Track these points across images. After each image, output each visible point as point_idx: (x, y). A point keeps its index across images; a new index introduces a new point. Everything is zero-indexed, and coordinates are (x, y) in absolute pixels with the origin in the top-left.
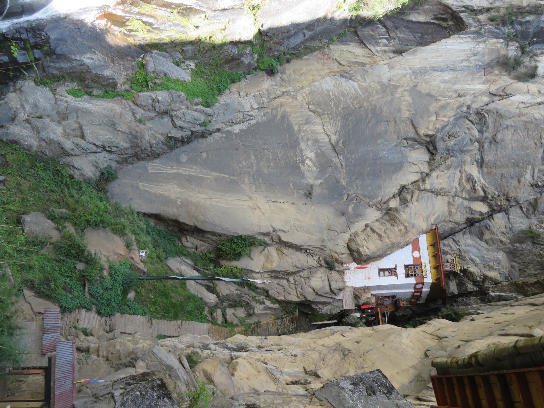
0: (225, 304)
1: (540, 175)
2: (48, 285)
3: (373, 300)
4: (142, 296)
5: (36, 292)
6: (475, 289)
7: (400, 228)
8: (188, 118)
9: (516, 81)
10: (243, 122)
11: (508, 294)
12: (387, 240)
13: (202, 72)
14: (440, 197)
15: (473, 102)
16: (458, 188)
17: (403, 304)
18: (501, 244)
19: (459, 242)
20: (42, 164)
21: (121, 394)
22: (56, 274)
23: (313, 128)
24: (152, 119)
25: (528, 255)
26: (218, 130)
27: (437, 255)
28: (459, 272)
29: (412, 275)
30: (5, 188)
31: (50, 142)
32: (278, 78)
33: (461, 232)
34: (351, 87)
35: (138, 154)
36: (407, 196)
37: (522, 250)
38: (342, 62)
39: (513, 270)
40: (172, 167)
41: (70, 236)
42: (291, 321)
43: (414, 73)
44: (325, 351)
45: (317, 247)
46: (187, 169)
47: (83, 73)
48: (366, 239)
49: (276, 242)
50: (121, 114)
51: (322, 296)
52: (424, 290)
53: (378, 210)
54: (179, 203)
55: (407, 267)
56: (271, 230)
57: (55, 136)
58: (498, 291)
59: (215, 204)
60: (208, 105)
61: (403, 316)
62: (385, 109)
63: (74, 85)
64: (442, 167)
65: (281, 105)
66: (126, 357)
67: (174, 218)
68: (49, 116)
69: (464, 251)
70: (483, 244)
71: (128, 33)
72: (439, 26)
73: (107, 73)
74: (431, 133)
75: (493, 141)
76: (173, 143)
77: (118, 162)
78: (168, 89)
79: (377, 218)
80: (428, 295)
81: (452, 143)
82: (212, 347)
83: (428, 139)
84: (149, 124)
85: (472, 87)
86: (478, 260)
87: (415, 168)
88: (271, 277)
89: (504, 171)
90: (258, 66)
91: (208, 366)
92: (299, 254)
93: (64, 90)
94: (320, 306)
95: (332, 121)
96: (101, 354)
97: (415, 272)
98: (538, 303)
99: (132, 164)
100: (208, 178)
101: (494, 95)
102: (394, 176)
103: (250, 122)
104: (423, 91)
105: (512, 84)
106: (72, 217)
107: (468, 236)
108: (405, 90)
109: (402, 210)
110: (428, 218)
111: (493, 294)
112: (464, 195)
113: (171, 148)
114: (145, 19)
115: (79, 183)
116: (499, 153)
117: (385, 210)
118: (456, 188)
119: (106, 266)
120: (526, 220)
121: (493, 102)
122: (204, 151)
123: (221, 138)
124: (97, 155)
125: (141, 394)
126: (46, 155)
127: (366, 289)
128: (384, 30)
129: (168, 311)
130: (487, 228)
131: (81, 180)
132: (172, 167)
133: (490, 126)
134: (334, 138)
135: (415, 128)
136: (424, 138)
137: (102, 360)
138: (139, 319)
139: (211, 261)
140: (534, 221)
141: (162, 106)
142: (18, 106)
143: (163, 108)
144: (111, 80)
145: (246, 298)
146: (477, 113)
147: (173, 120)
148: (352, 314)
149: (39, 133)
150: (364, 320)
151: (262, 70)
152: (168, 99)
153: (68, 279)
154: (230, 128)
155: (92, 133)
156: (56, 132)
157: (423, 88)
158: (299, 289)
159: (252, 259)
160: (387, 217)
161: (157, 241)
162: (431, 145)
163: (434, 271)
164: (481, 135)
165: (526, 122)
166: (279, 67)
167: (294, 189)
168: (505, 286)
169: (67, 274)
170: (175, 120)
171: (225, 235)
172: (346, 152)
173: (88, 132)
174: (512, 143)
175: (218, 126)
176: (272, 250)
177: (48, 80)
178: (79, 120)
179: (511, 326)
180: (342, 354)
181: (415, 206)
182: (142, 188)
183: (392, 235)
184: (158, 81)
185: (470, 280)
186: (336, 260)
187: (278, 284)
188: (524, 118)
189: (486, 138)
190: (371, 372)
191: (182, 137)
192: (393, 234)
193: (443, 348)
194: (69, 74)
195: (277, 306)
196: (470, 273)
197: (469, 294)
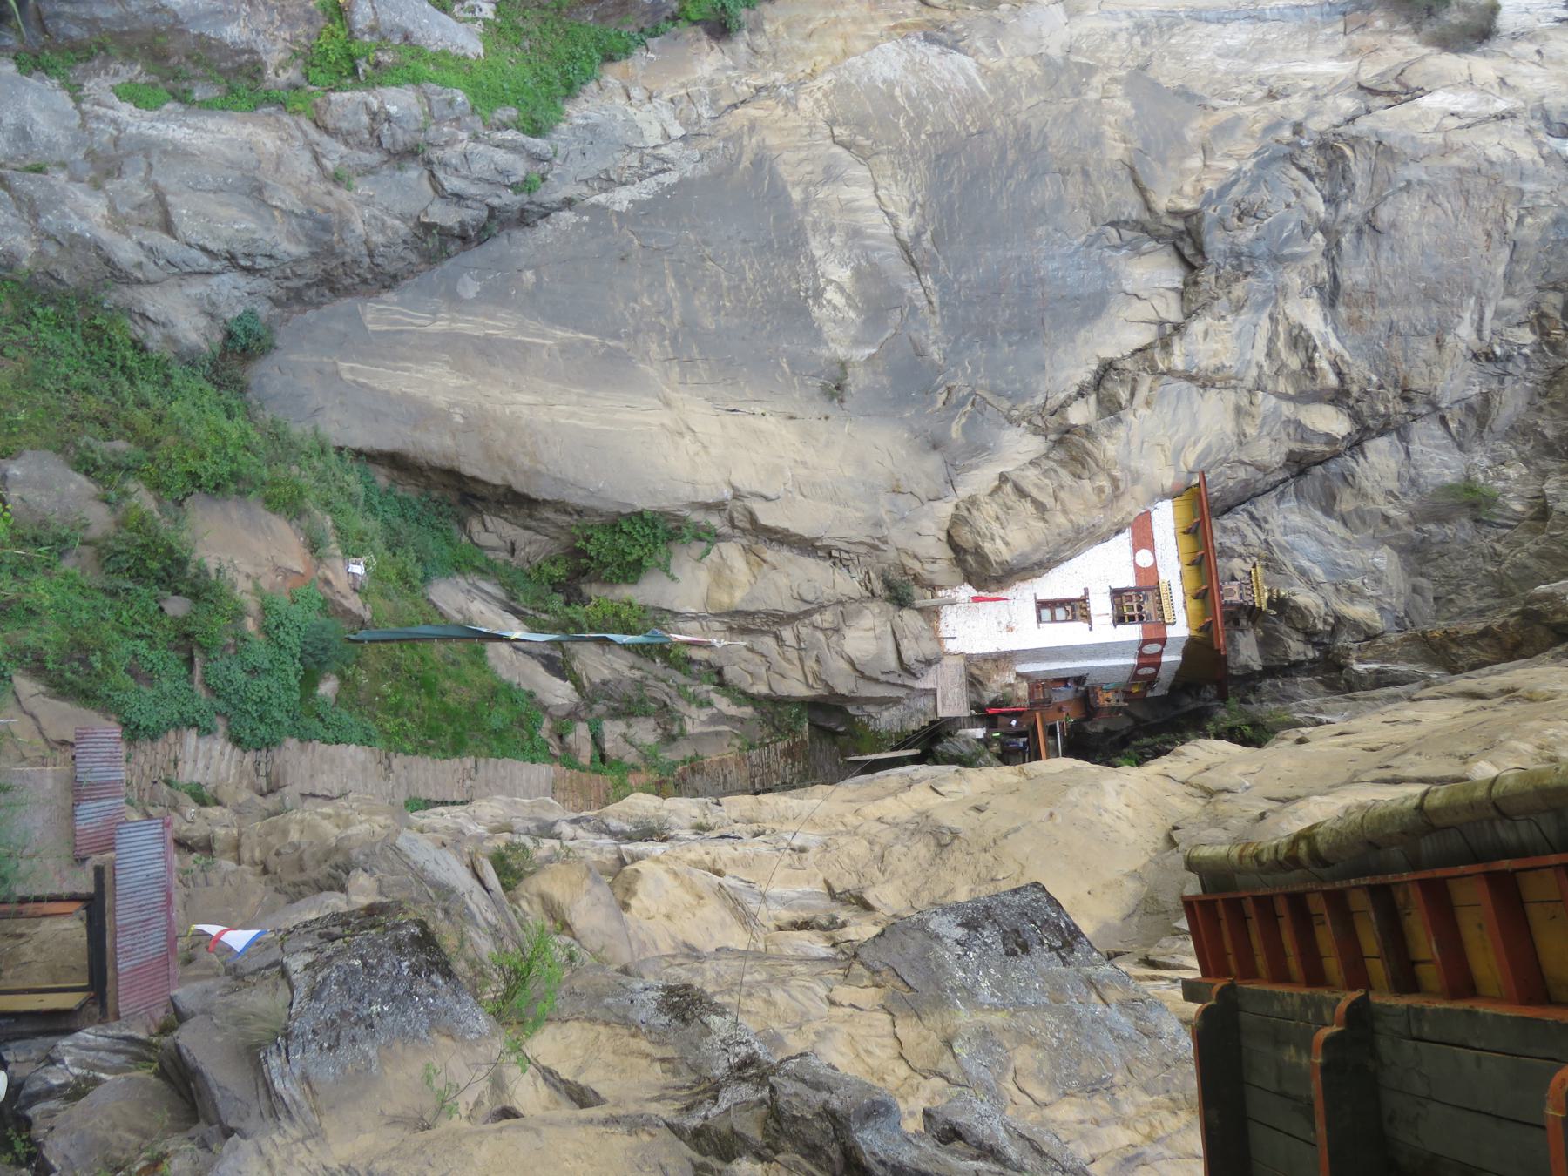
0: (599, 708)
1: (1498, 325)
2: (85, 662)
3: (1023, 690)
4: (358, 688)
5: (51, 684)
6: (1310, 655)
7: (1098, 483)
8: (478, 167)
9: (1436, 50)
10: (641, 178)
11: (1404, 668)
12: (1061, 519)
13: (516, 29)
14: (1212, 393)
15: (1312, 113)
16: (1266, 365)
17: (1106, 699)
18: (1384, 527)
19: (1266, 522)
20: (51, 309)
21: (307, 967)
22: (107, 631)
23: (847, 193)
24: (370, 171)
25: (1462, 557)
26: (568, 203)
27: (1202, 560)
28: (1264, 607)
29: (1132, 619)
31: (72, 243)
32: (742, 47)
33: (1273, 494)
34: (955, 70)
35: (334, 276)
37: (1443, 542)
39: (1418, 598)
41: (142, 521)
42: (790, 753)
43: (1140, 27)
44: (886, 835)
45: (861, 543)
46: (481, 320)
47: (162, 34)
48: (1003, 516)
49: (743, 530)
50: (279, 157)
51: (877, 681)
52: (1165, 659)
53: (1035, 434)
54: (458, 419)
55: (1117, 594)
56: (727, 493)
57: (85, 225)
58: (1375, 659)
59: (563, 421)
60: (536, 131)
61: (1107, 733)
62: (1055, 136)
64: (1221, 306)
66: (319, 863)
67: (446, 464)
68: (63, 165)
69: (1279, 545)
70: (1334, 525)
73: (234, 32)
74: (1188, 206)
75: (1366, 228)
76: (437, 245)
77: (275, 302)
78: (415, 81)
79: (1033, 456)
80: (1177, 673)
81: (1250, 234)
82: (566, 829)
83: (1179, 225)
84: (364, 188)
85: (1309, 68)
86: (1318, 573)
87: (1141, 310)
88: (731, 629)
89: (1397, 314)
90: (683, 10)
91: (553, 883)
92: (808, 562)
93: (106, 85)
94: (871, 709)
95: (901, 173)
96: (246, 855)
97: (1140, 608)
98: (1486, 689)
99: (318, 305)
100: (543, 345)
101: (1373, 92)
102: (1082, 332)
103: (661, 177)
104: (1166, 82)
105: (1422, 58)
106: (146, 465)
107: (1291, 503)
108: (1114, 80)
109: (1104, 430)
110: (1178, 453)
111: (1359, 667)
112: (1283, 386)
113: (432, 259)
115: (161, 365)
116: (1383, 262)
117: (1056, 431)
118: (1260, 367)
119: (252, 604)
120: (1457, 455)
121: (1368, 112)
122: (528, 267)
123: (577, 225)
125: (365, 965)
126: (61, 282)
127: (1002, 659)
129: (434, 732)
130: (1346, 480)
131: (168, 354)
133: (1359, 183)
134: (907, 224)
135: (1142, 191)
136: (1168, 221)
137: (249, 874)
138: (354, 755)
139: (556, 587)
140: (1480, 458)
141: (399, 132)
143: (403, 138)
145: (659, 691)
146: (1323, 146)
147: (432, 175)
148: (961, 732)
149: (36, 216)
150: (996, 748)
151: (695, 23)
152: (417, 110)
153: (141, 645)
154: (601, 198)
155: (197, 214)
156: (88, 212)
157: (1167, 73)
158: (811, 663)
159: (674, 579)
160: (1059, 454)
161: (396, 533)
162: (1189, 240)
163: (1194, 605)
164: (1332, 210)
165: (1462, 171)
166: (744, 14)
167: (793, 373)
168: (1395, 645)
169: (138, 630)
170: (440, 175)
171: (596, 512)
172: (942, 266)
173: (182, 212)
174: (1419, 234)
175: (568, 191)
176: (732, 552)
178: (154, 177)
179: (1411, 756)
180: (933, 842)
181: (1140, 420)
182: (347, 376)
183: (1074, 506)
184: (385, 58)
185: (1297, 630)
186: (916, 578)
187: (751, 650)
188: (1455, 160)
189: (1347, 219)
190: (1015, 891)
191: (462, 224)
192: (1079, 501)
193: (1217, 821)
194: (118, 37)
195: (747, 711)
196: (1297, 608)
197: (1290, 669)
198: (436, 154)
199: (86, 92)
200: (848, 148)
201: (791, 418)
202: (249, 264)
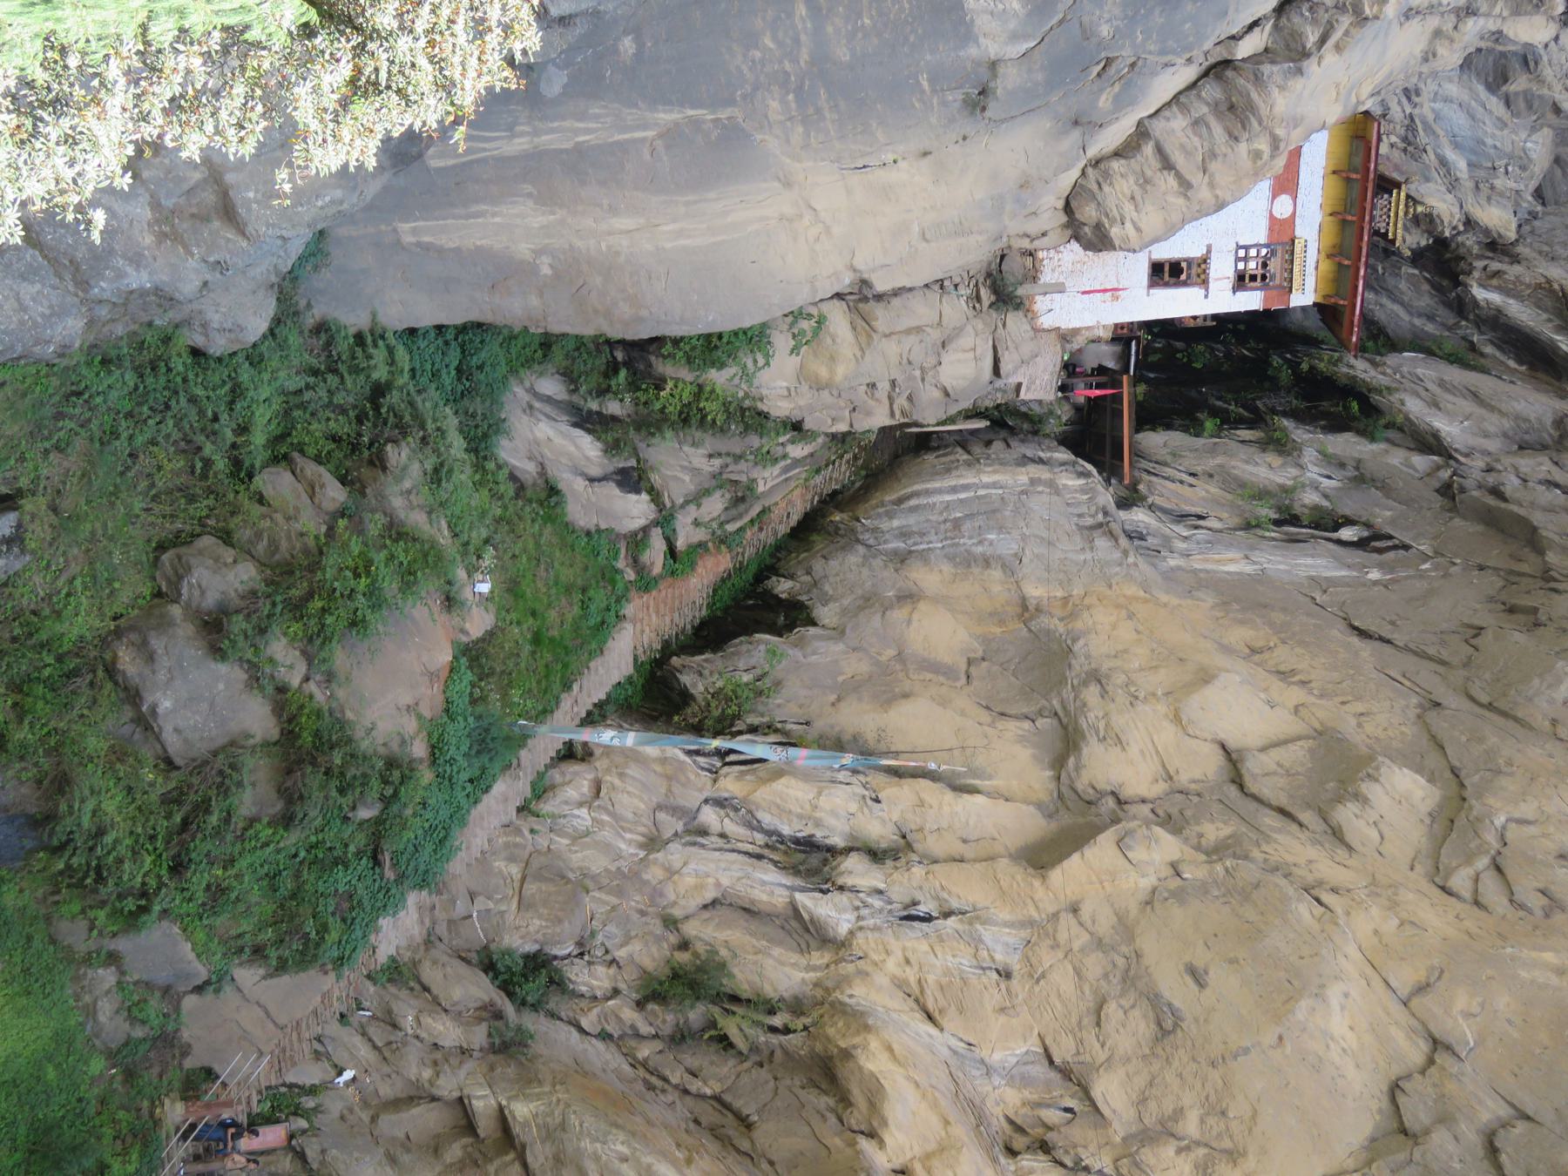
7: (1256, 146)
36: (1309, 29)
40: (510, 128)
48: (1138, 198)
54: (546, 270)
58: (1499, 289)
59: (668, 245)
69: (1425, 123)
70: (1495, 104)
86: (1460, 164)
100: (643, 140)
109: (1278, 79)
111: (1480, 293)
130: (1526, 62)
132: (510, 128)
149: (83, 284)
160: (1211, 90)
163: (1326, 266)
167: (934, 91)
182: (408, 239)
201: (925, 154)
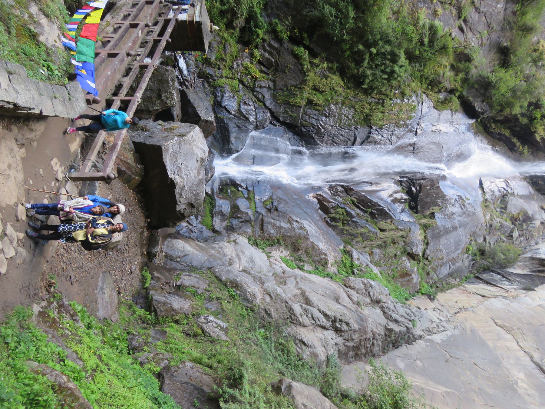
20: (262, 330)
24: (366, 305)
26: (420, 337)
30: (228, 339)
38: (485, 295)
47: (299, 237)
63: (286, 253)
65: (466, 320)
71: (330, 222)
72: (538, 276)
73: (322, 245)
114: (348, 209)
124: (326, 332)
126: (269, 315)
128: (499, 276)
142: (234, 255)
144: (323, 256)
147: (384, 313)
149: (263, 283)
151: (423, 294)
177: (265, 240)
178: (300, 286)
191: (400, 331)
194: (284, 237)
198: (384, 305)
199: (272, 255)
200: (501, 327)
202: (339, 326)
